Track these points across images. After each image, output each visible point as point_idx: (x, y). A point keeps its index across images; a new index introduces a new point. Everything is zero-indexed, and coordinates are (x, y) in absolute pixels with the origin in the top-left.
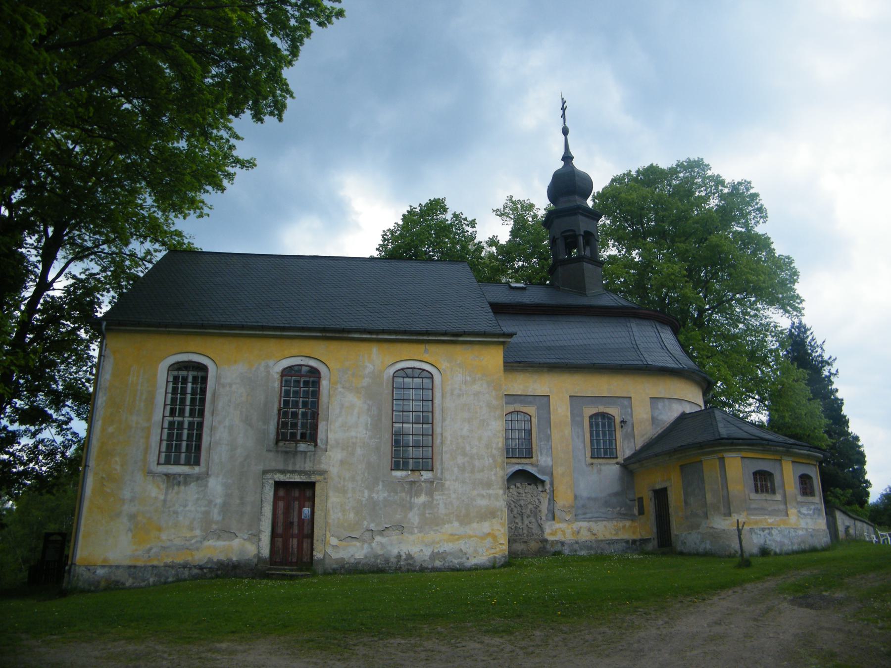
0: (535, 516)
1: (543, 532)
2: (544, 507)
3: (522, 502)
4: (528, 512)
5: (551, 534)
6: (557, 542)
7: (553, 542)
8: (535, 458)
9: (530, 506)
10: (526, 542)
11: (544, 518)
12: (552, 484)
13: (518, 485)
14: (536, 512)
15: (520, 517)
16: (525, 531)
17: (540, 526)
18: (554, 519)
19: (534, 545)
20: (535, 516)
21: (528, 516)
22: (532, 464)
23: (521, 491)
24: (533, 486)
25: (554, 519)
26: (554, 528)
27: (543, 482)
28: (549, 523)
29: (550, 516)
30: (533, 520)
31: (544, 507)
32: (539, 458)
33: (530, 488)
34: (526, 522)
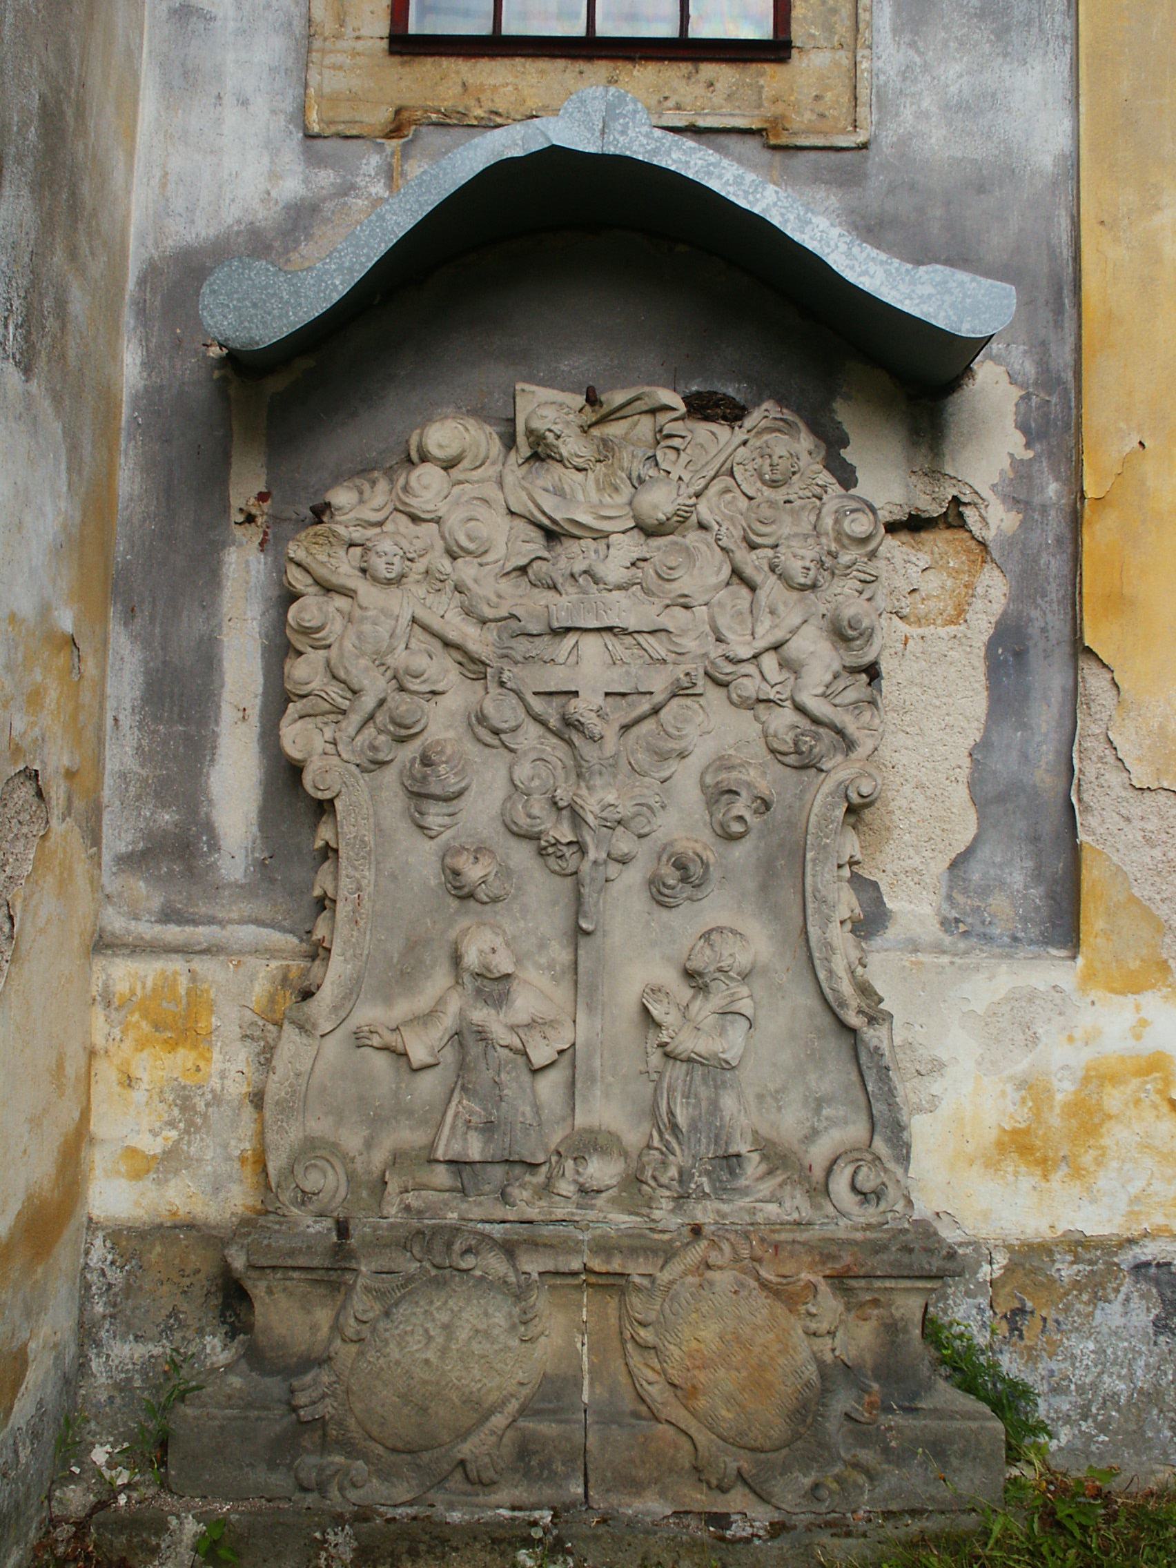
0: (784, 868)
1: (889, 1129)
2: (931, 730)
3: (590, 668)
4: (682, 822)
5: (1022, 1147)
6: (1101, 1264)
7: (1029, 1258)
8: (813, 64)
9: (714, 731)
10: (613, 1285)
11: (914, 907)
12: (1057, 425)
13: (546, 406)
14: (797, 820)
15: (540, 891)
16: (605, 1111)
17: (850, 1032)
18: (1062, 919)
19: (731, 1346)
20: (784, 868)
21: (678, 880)
22: (770, 140)
23: (581, 497)
24: (770, 439)
25: (1062, 919)
26: (1061, 1059)
27: (915, 376)
28: (997, 981)
29: (1015, 882)
30: (756, 942)
31: (931, 730)
32: (887, 55)
33: (743, 467)
34: (640, 954)
